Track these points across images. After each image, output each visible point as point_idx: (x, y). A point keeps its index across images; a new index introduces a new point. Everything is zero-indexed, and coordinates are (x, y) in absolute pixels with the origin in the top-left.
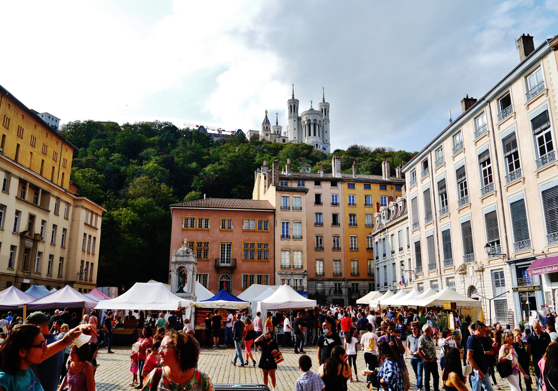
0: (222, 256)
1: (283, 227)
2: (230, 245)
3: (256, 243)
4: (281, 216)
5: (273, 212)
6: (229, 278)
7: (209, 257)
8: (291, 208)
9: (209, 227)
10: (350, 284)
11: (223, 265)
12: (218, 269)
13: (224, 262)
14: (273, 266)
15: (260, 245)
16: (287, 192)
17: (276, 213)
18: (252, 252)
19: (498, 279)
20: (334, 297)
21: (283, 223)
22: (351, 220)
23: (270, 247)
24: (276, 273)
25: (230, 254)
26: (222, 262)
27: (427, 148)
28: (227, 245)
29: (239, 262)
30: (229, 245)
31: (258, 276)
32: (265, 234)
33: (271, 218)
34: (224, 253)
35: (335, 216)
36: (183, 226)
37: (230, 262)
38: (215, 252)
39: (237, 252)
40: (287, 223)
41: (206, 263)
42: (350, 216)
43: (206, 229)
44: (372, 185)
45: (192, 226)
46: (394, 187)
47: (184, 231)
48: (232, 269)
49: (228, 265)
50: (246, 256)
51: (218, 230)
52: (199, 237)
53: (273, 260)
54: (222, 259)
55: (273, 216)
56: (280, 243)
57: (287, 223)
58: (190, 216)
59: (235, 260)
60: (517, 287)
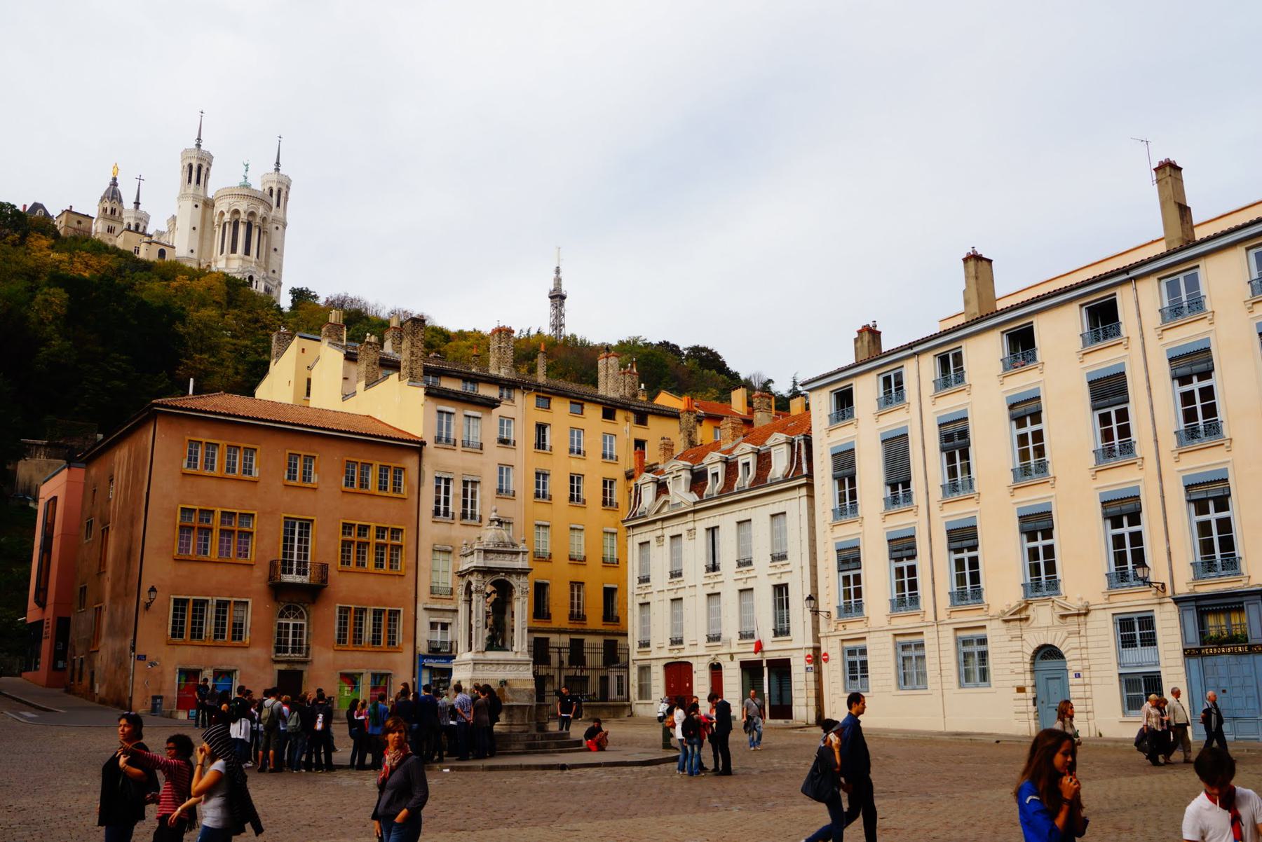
0: (285, 555)
1: (438, 488)
2: (307, 527)
3: (373, 525)
4: (437, 460)
5: (416, 447)
6: (302, 617)
7: (252, 557)
8: (459, 443)
9: (256, 473)
10: (565, 639)
11: (288, 578)
12: (278, 591)
13: (291, 572)
14: (412, 589)
15: (381, 531)
16: (449, 403)
17: (425, 451)
18: (362, 546)
19: (1137, 631)
20: (571, 673)
21: (438, 479)
22: (538, 485)
23: (404, 539)
24: (420, 607)
25: (306, 549)
26: (284, 572)
27: (911, 348)
28: (301, 526)
29: (332, 572)
30: (306, 525)
31: (375, 611)
32: (398, 503)
33: (410, 463)
34: (292, 548)
35: (541, 475)
36: (185, 465)
37: (305, 574)
38: (266, 542)
39: (324, 545)
40: (447, 481)
41: (245, 570)
42: (538, 474)
43: (247, 477)
44: (586, 406)
45: (209, 464)
46: (632, 416)
47: (189, 479)
48: (314, 593)
49: (304, 579)
50: (345, 560)
51: (279, 484)
52: (229, 498)
53: (412, 572)
54: (284, 562)
55: (416, 458)
56: (431, 532)
57: (447, 481)
58: (204, 435)
59: (324, 568)
60: (1198, 646)
